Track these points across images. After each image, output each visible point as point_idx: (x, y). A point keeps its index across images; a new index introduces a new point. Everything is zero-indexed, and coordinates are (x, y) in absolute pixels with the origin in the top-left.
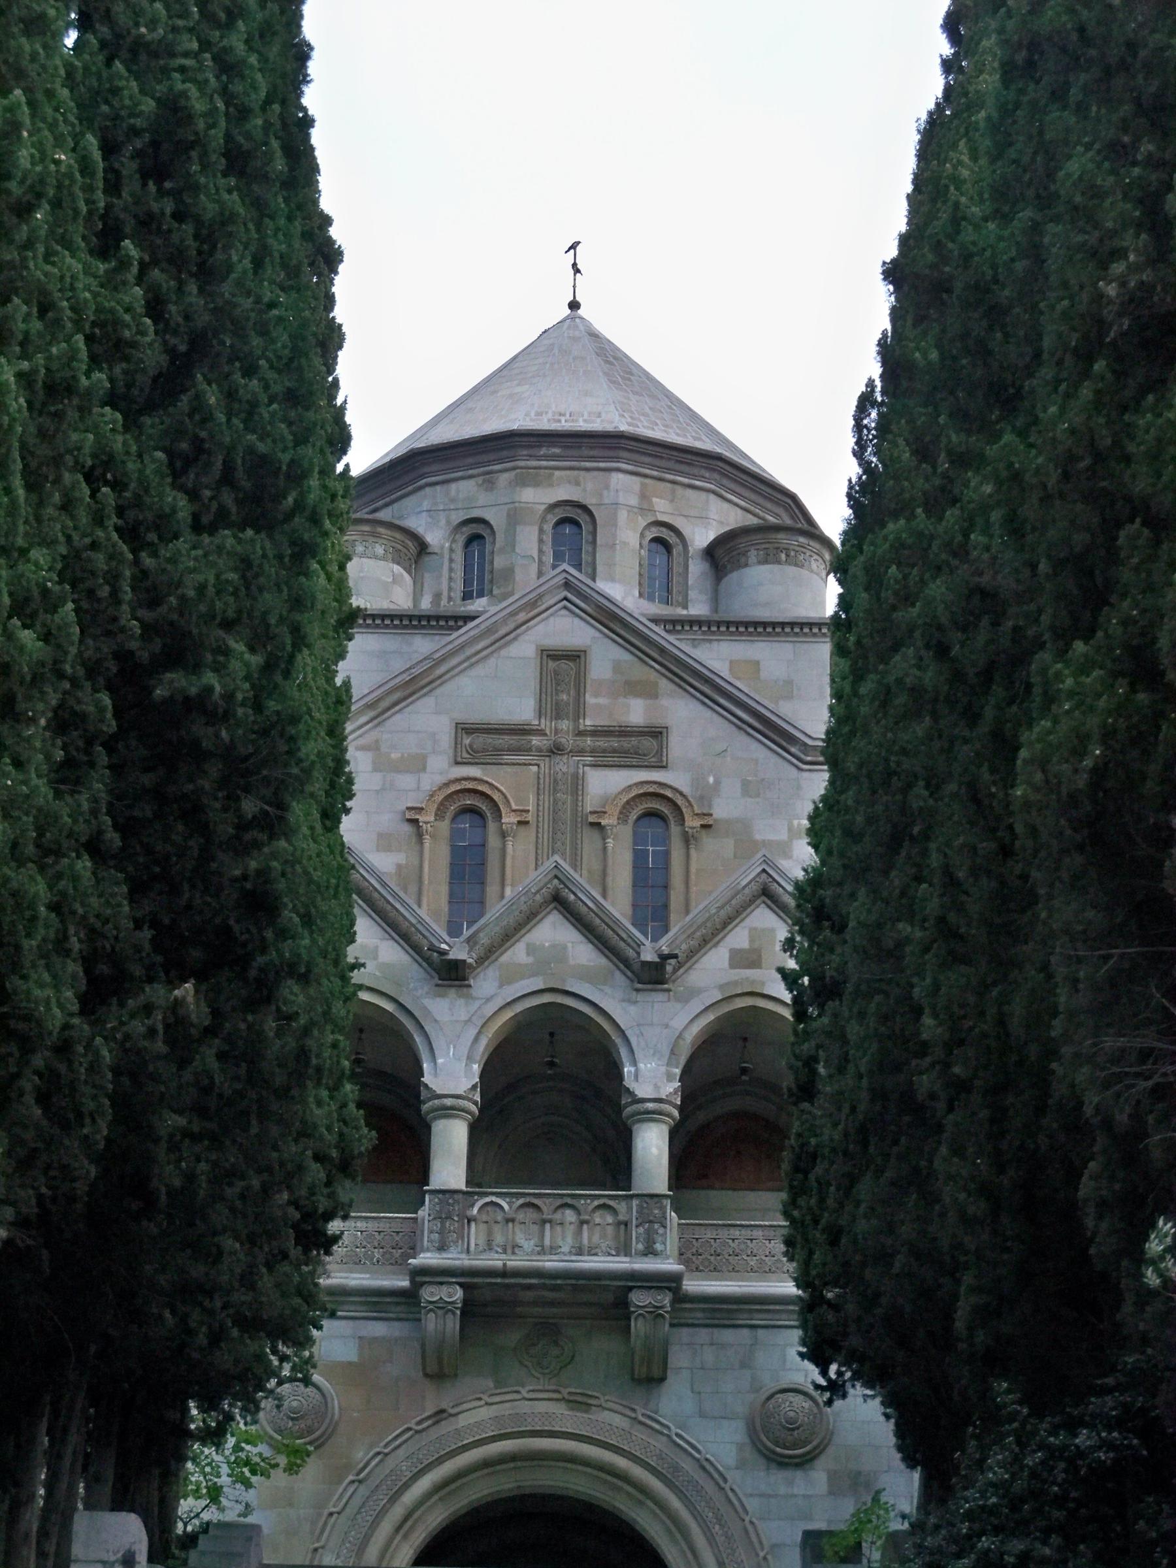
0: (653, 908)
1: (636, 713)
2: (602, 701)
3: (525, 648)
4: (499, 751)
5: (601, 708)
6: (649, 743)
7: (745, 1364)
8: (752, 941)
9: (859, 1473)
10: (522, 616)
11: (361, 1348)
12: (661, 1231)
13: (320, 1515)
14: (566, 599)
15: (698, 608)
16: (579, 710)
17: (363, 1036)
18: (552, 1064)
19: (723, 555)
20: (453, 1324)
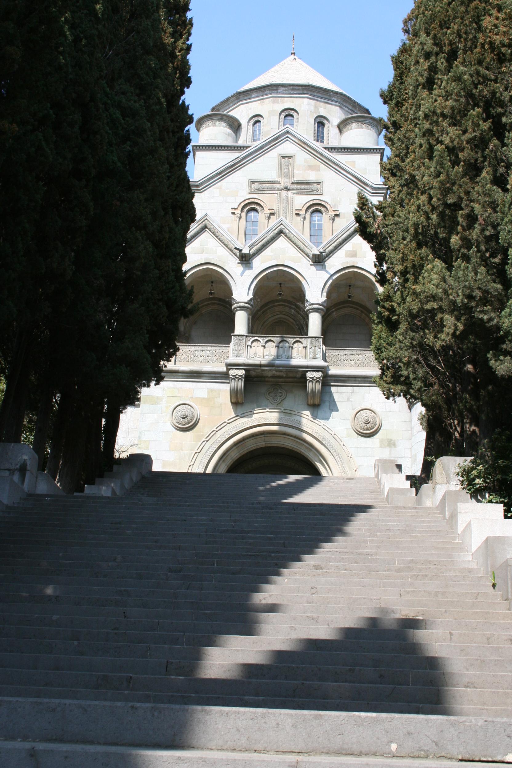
1: (312, 176)
4: (263, 189)
7: (348, 400)
9: (391, 440)
11: (208, 393)
12: (319, 350)
13: (192, 453)
14: (288, 137)
17: (213, 284)
18: (280, 295)
20: (241, 384)
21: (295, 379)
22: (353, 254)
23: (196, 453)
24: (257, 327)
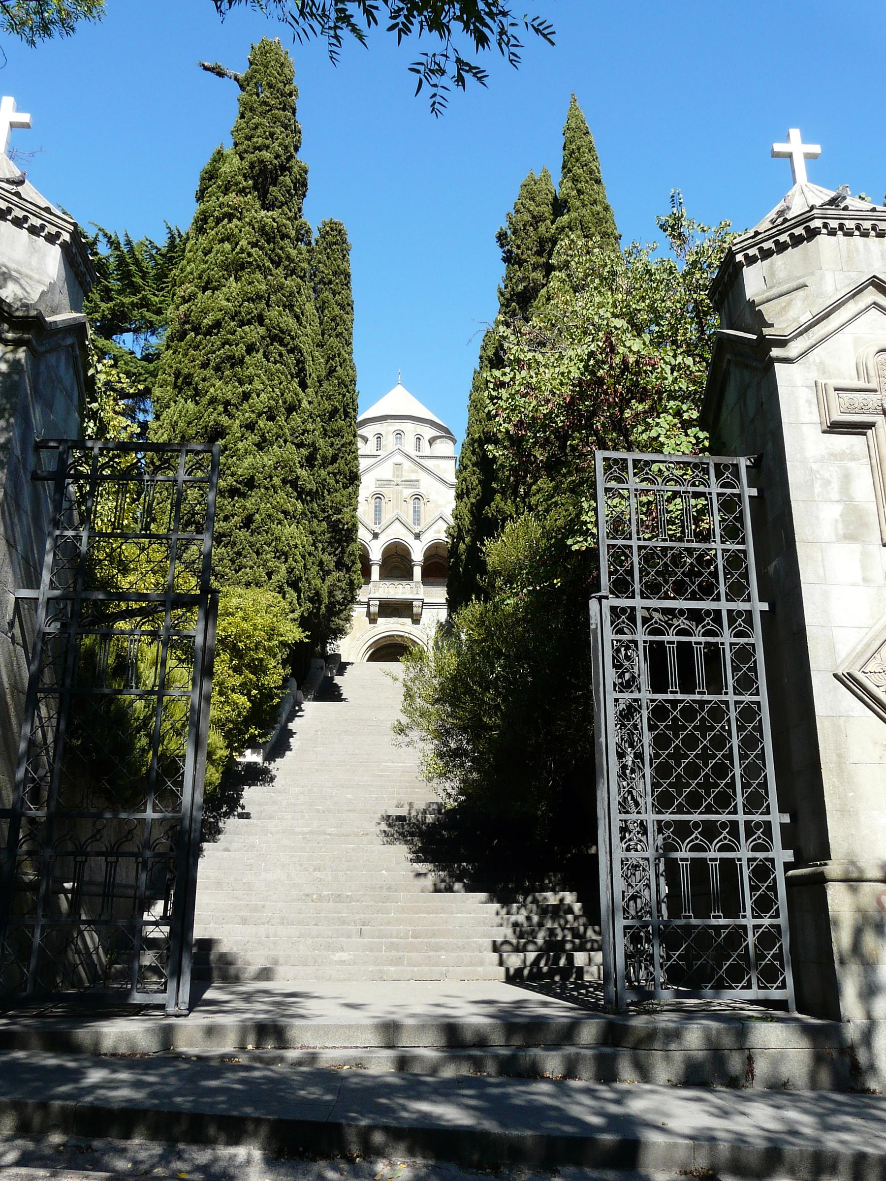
0: (417, 520)
1: (413, 477)
5: (407, 476)
15: (428, 453)
16: (402, 477)
19: (432, 441)
20: (377, 609)
24: (384, 576)
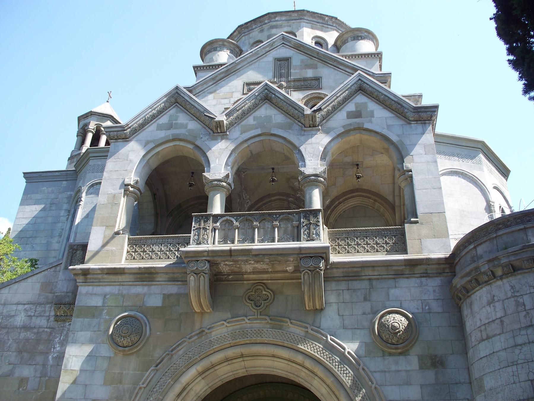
1: (310, 73)
2: (296, 71)
3: (270, 58)
5: (295, 73)
6: (314, 82)
8: (356, 107)
9: (436, 356)
10: (268, 49)
11: (164, 299)
13: (135, 388)
16: (288, 74)
18: (273, 181)
21: (287, 274)
22: (357, 114)
23: (140, 388)
